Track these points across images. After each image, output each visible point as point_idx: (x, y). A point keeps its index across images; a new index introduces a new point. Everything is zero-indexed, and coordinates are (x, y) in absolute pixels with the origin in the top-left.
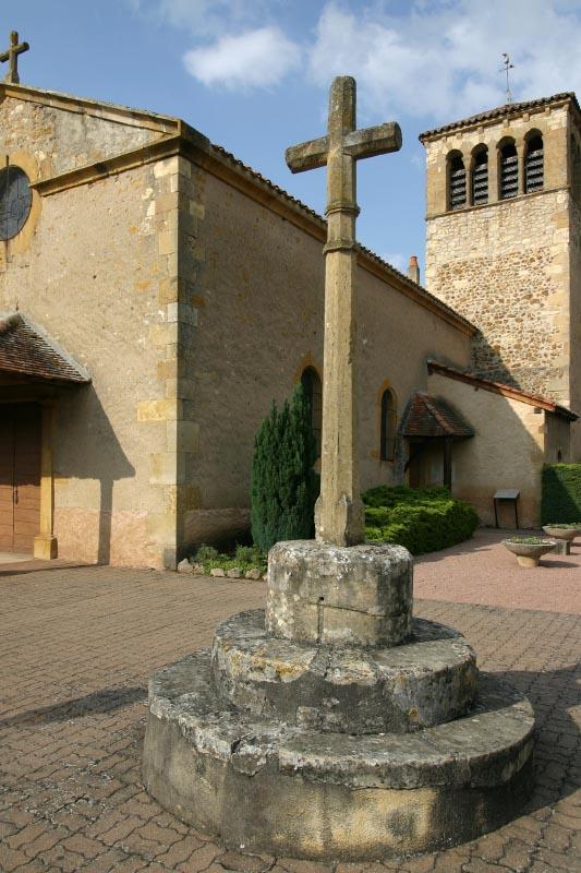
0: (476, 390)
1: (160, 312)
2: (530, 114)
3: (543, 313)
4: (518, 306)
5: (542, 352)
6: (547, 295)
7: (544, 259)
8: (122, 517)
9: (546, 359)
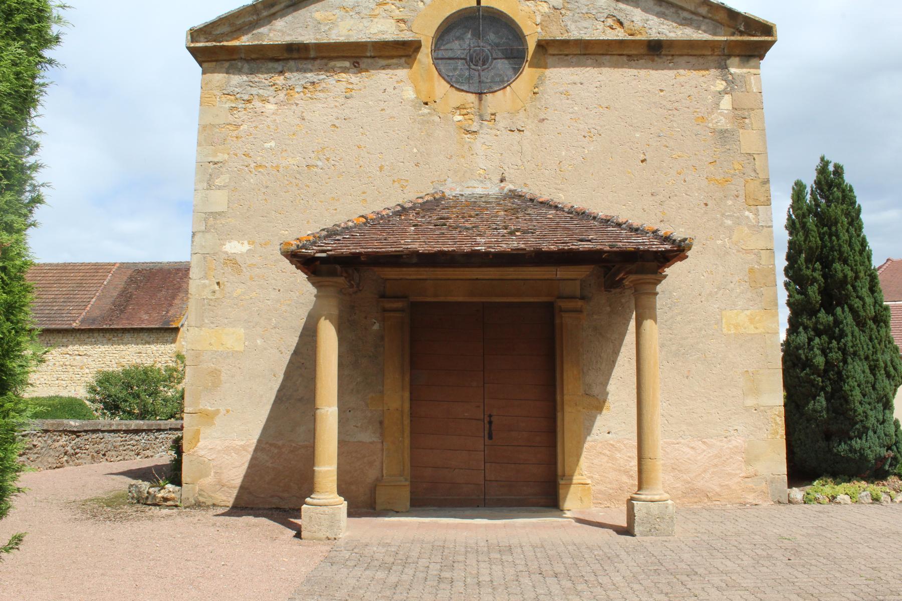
1: (747, 213)
8: (704, 447)
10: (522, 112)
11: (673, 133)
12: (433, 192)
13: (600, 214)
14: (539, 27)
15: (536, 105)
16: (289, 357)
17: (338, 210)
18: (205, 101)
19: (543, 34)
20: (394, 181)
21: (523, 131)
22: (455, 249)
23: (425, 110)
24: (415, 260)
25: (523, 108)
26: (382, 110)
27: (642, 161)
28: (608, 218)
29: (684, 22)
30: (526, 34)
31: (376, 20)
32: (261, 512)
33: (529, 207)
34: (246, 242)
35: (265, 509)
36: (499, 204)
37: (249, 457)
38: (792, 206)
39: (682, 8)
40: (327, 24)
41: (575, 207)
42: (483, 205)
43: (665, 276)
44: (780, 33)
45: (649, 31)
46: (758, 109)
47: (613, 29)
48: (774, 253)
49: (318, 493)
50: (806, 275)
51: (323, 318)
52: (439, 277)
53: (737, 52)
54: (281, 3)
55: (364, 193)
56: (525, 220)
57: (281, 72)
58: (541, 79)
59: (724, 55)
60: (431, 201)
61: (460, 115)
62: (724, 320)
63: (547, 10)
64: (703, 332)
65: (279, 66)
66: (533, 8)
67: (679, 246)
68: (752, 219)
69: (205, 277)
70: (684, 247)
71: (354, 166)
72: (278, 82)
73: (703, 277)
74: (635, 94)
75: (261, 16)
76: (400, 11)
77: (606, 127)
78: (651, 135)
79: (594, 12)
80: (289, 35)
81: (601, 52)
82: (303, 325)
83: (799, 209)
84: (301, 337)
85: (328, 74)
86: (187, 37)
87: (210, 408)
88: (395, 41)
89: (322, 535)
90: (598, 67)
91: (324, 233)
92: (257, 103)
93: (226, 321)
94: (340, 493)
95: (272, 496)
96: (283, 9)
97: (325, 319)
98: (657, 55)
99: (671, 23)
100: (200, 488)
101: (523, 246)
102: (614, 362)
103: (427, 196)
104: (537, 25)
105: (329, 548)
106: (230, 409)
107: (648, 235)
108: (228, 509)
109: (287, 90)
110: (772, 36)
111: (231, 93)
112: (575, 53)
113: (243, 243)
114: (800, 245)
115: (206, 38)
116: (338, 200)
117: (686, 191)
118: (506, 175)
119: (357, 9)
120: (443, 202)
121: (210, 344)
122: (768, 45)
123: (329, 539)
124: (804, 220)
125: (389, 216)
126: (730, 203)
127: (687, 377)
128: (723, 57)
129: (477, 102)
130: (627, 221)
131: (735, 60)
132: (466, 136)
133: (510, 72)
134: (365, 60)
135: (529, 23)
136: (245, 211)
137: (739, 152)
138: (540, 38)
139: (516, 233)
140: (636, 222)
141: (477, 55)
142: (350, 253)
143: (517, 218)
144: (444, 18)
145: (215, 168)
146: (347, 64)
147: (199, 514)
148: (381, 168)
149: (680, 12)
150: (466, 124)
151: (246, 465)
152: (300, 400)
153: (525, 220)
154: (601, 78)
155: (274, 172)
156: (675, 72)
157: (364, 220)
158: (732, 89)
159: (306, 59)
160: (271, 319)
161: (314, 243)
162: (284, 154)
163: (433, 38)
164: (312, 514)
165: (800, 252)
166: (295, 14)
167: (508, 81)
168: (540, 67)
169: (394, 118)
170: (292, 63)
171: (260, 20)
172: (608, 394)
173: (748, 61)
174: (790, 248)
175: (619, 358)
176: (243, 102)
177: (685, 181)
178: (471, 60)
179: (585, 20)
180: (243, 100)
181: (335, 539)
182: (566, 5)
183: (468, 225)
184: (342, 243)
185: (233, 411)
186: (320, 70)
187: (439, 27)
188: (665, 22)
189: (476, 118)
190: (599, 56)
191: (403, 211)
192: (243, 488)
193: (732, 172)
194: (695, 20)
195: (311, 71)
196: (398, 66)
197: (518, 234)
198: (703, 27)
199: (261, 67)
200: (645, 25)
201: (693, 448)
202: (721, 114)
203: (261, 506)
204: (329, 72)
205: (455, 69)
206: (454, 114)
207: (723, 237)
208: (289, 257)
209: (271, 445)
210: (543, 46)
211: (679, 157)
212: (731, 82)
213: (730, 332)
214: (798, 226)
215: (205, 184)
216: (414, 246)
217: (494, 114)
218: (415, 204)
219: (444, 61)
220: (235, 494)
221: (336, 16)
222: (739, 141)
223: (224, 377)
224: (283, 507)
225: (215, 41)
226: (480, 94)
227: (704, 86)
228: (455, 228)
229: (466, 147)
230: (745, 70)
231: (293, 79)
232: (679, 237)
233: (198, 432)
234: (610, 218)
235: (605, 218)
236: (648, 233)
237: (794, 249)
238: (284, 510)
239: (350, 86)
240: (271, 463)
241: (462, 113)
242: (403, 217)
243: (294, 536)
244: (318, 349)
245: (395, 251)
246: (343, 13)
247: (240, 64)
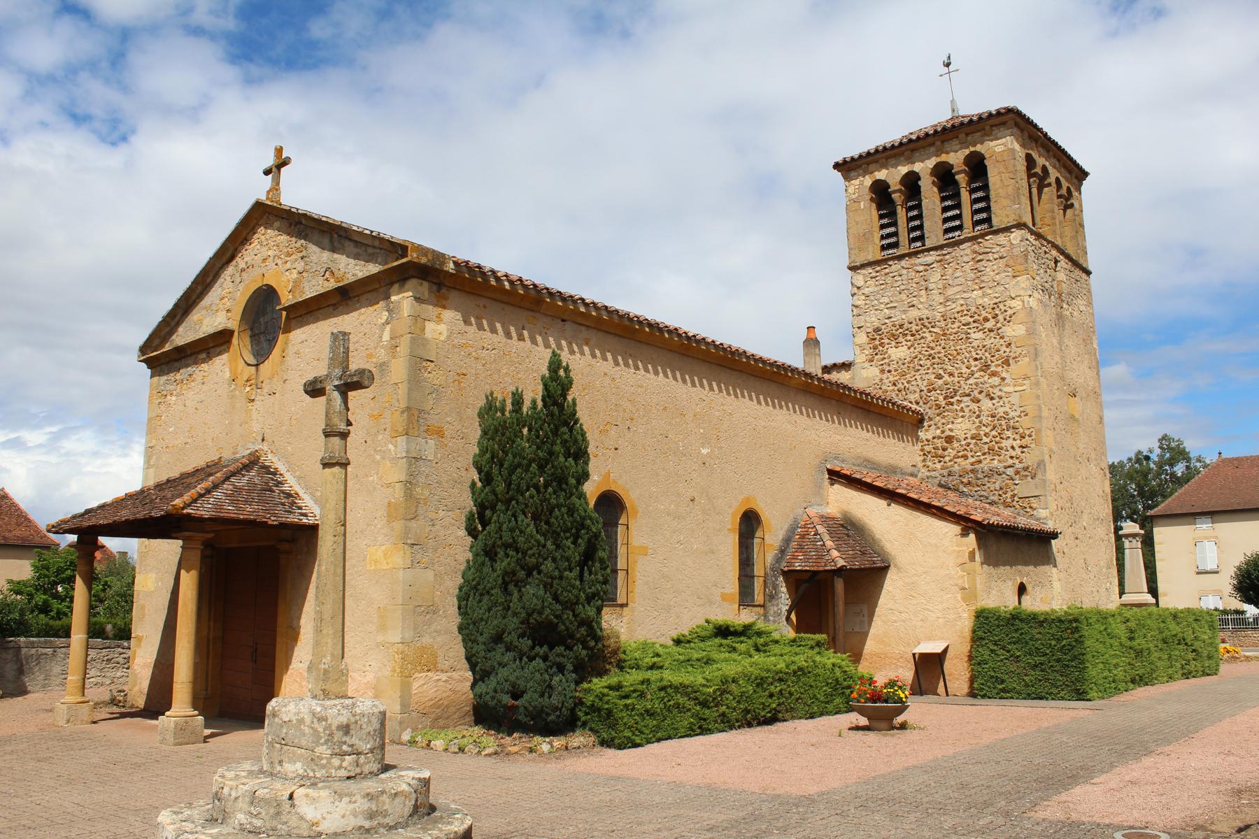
0: (889, 505)
2: (967, 135)
3: (1006, 389)
4: (972, 381)
5: (1005, 444)
6: (1009, 365)
7: (1001, 318)
9: (1014, 454)
39: (369, 246)
126: (380, 437)
146: (204, 355)
159: (188, 356)
173: (404, 285)
202: (382, 347)
206: (245, 386)
230: (401, 296)
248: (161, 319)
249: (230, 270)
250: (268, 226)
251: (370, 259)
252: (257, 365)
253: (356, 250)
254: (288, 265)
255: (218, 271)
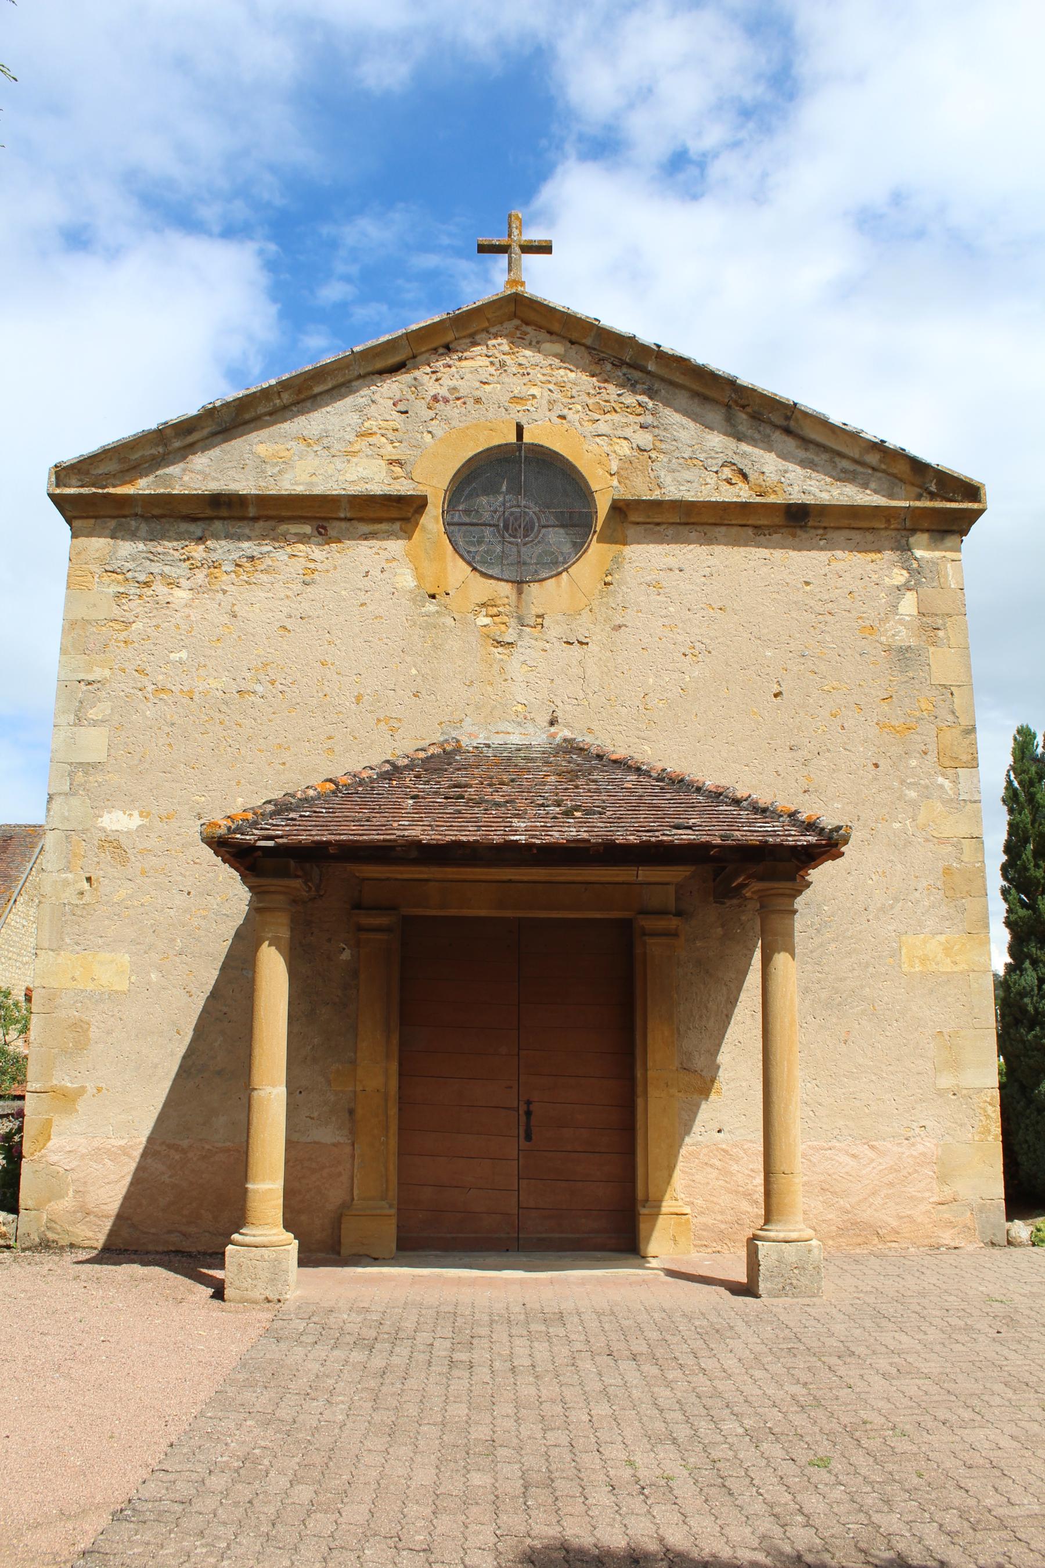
1: (940, 780)
8: (871, 1154)
10: (585, 613)
11: (824, 650)
12: (442, 739)
13: (708, 783)
14: (615, 478)
15: (608, 602)
16: (202, 1003)
17: (288, 765)
18: (75, 582)
19: (622, 489)
20: (379, 720)
21: (587, 644)
22: (478, 838)
23: (431, 607)
24: (414, 854)
25: (588, 608)
26: (362, 605)
27: (776, 695)
28: (720, 790)
29: (842, 475)
30: (593, 490)
31: (354, 460)
32: (151, 1257)
33: (595, 768)
34: (136, 813)
35: (157, 1253)
36: (547, 763)
37: (133, 1166)
38: (1013, 768)
39: (840, 455)
40: (276, 464)
41: (669, 770)
42: (522, 763)
43: (808, 885)
44: (992, 497)
45: (789, 488)
46: (957, 615)
47: (731, 484)
48: (983, 843)
49: (251, 1226)
50: (1036, 877)
51: (267, 943)
52: (450, 877)
53: (926, 525)
54: (203, 428)
55: (330, 738)
56: (589, 791)
57: (201, 539)
58: (617, 561)
59: (905, 529)
60: (439, 756)
61: (487, 616)
62: (904, 951)
63: (628, 452)
64: (871, 969)
65: (196, 529)
66: (606, 449)
67: (830, 839)
68: (948, 789)
69: (68, 869)
70: (837, 840)
71: (315, 694)
72: (194, 554)
73: (870, 882)
74: (764, 588)
75: (170, 448)
76: (394, 447)
77: (720, 640)
78: (791, 654)
79: (702, 457)
80: (214, 479)
81: (712, 521)
82: (227, 950)
83: (1024, 772)
84: (223, 969)
85: (277, 545)
86: (49, 478)
87: (69, 1085)
88: (385, 495)
89: (258, 1294)
90: (708, 545)
91: (270, 808)
92: (160, 588)
93: (100, 941)
94: (287, 1227)
95: (170, 1232)
96: (207, 438)
97: (270, 945)
98: (801, 527)
99: (823, 477)
100: (50, 1217)
101: (585, 835)
102: (728, 1017)
103: (432, 747)
104: (611, 475)
105: (270, 1316)
106: (104, 1086)
107: (781, 819)
108: (96, 1252)
109: (209, 567)
110: (979, 502)
111: (119, 570)
112: (671, 521)
113: (130, 815)
114: (1025, 830)
115: (79, 480)
116: (289, 748)
117: (845, 743)
118: (559, 714)
119: (325, 441)
120: (458, 758)
121: (73, 979)
122: (973, 516)
123: (269, 1301)
124: (1032, 790)
125: (372, 781)
126: (913, 763)
127: (845, 1042)
128: (904, 533)
129: (513, 597)
130: (750, 796)
131: (924, 537)
132: (495, 650)
133: (567, 548)
134: (336, 524)
135: (600, 472)
136: (136, 762)
137: (929, 682)
138: (616, 497)
139: (575, 813)
140: (764, 798)
141: (516, 519)
142: (313, 842)
143: (577, 787)
144: (464, 460)
145: (90, 691)
146: (307, 529)
147: (48, 1261)
148: (358, 699)
149: (837, 459)
150: (495, 631)
151: (128, 1179)
152: (220, 1073)
153: (589, 791)
154: (712, 561)
155: (186, 701)
156: (829, 554)
157: (333, 787)
158: (918, 583)
160: (174, 940)
161: (254, 824)
162: (202, 672)
163: (446, 491)
164: (242, 1259)
165: (1026, 841)
166: (225, 446)
167: (564, 563)
168: (616, 543)
169: (381, 617)
170: (218, 525)
171: (168, 454)
172: (718, 1067)
173: (942, 539)
174: (1010, 834)
175: (736, 1011)
176: (137, 585)
177: (843, 728)
178: (506, 527)
179: (688, 469)
180: (138, 582)
181: (279, 1301)
182: (658, 444)
183: (498, 798)
184: (299, 825)
185: (107, 1090)
186: (264, 537)
187: (455, 474)
188: (814, 475)
189: (513, 622)
190: (708, 527)
191: (393, 772)
192: (121, 1218)
193: (917, 714)
194: (861, 473)
195: (249, 538)
196: (389, 535)
197: (577, 814)
198: (873, 485)
199: (168, 530)
200: (783, 479)
201: (854, 1156)
202: (901, 622)
203: (150, 1248)
204: (278, 542)
205: (480, 542)
206: (476, 614)
207: (902, 818)
208: (215, 845)
209: (170, 1146)
210: (620, 509)
211: (833, 688)
212: (916, 572)
213: (913, 970)
214: (1022, 797)
215: (72, 717)
216: (413, 833)
217: (541, 616)
218: (413, 760)
219: (464, 528)
220: (109, 1228)
221: (292, 452)
222: (929, 665)
223: (94, 1033)
224: (187, 1250)
225: (93, 485)
226: (519, 584)
227: (874, 577)
228: (479, 803)
229: (496, 667)
230: (938, 554)
231: (220, 551)
232: (829, 824)
233: (49, 1123)
234: (722, 790)
235: (714, 790)
236: (782, 816)
237: (1017, 835)
238: (189, 1255)
239: (312, 565)
240: (170, 1177)
241: (490, 613)
242: (395, 782)
243: (212, 1297)
244: (256, 993)
245: (384, 840)
246: (302, 446)
247: (133, 523)
248: (154, 426)
249: (391, 387)
250: (518, 339)
251: (845, 477)
252: (520, 583)
253: (802, 454)
254: (602, 427)
255: (350, 381)
